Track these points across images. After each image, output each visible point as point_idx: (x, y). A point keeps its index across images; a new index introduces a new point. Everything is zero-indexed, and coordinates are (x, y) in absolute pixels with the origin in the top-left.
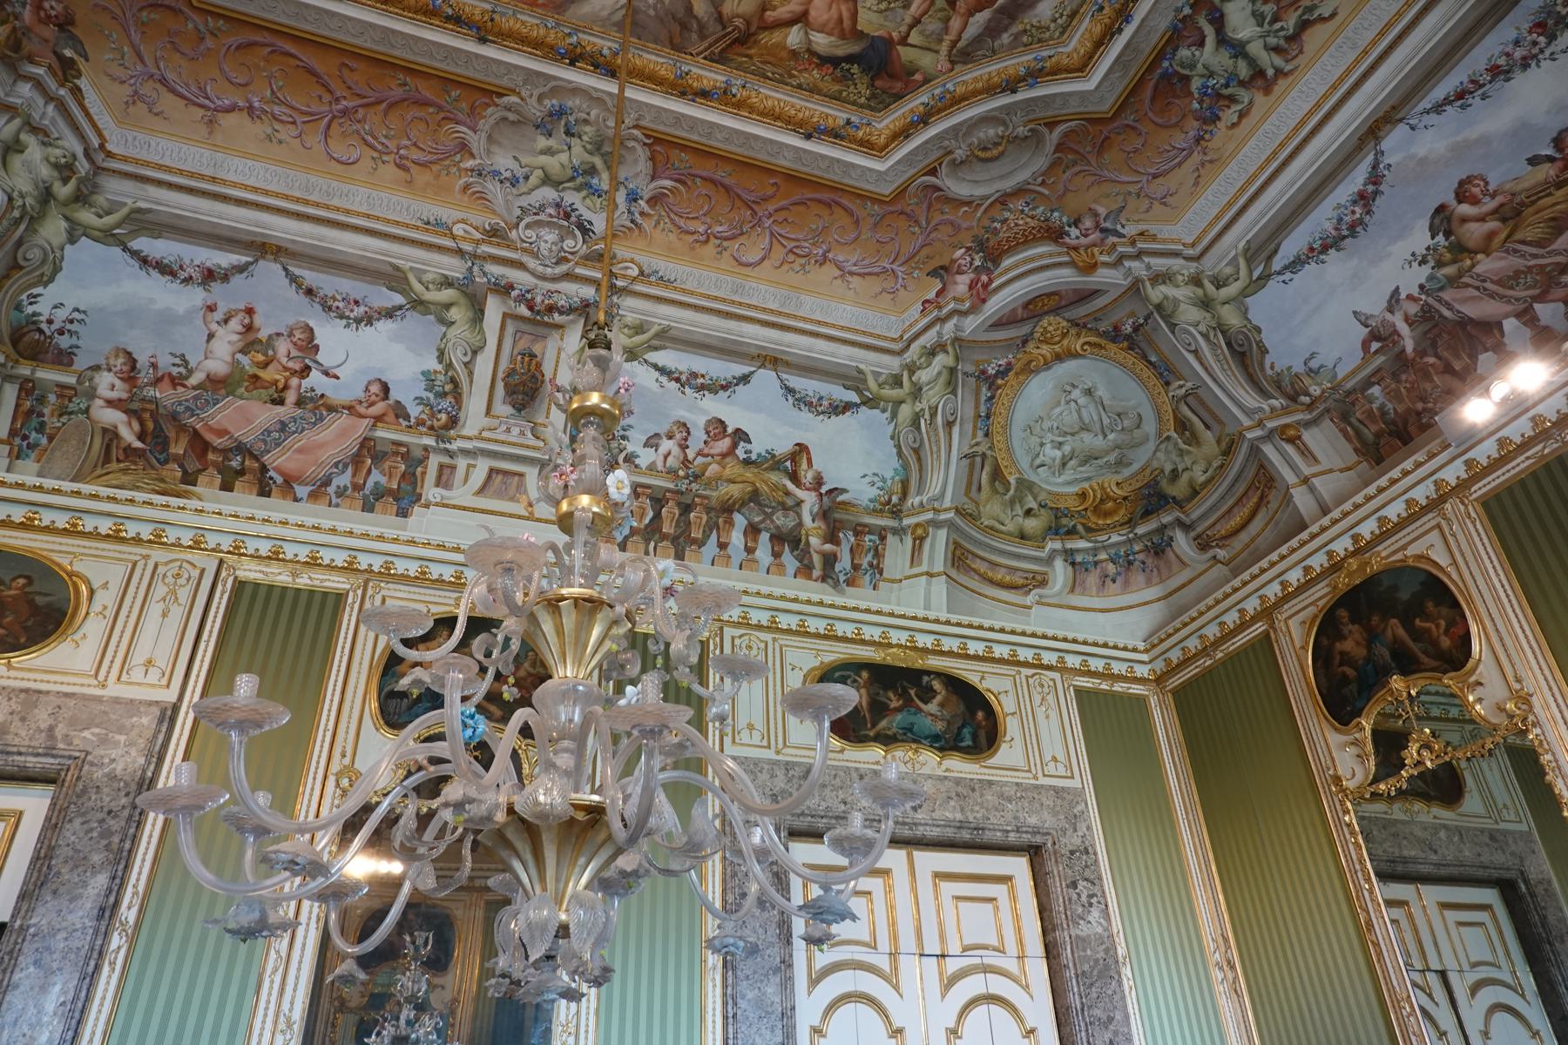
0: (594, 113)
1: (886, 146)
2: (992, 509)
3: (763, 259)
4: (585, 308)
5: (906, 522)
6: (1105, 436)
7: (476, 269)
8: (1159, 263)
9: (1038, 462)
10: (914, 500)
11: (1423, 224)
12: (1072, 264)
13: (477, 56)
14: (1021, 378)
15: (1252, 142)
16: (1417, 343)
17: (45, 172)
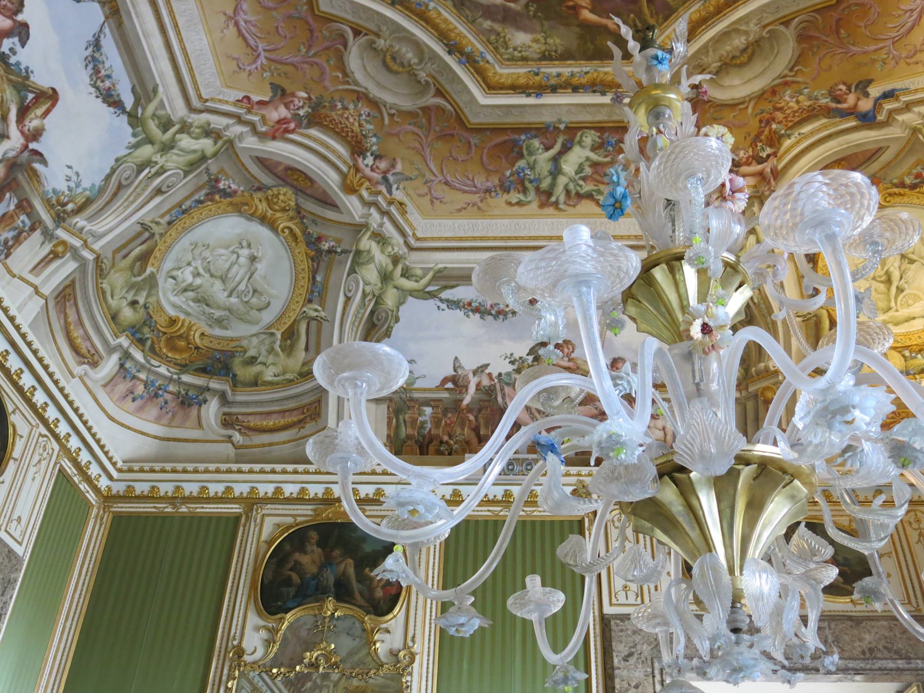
2: (117, 279)
5: (61, 233)
6: (230, 295)
8: (389, 229)
9: (175, 273)
10: (80, 221)
11: (531, 344)
12: (344, 176)
15: (506, 221)
16: (472, 402)
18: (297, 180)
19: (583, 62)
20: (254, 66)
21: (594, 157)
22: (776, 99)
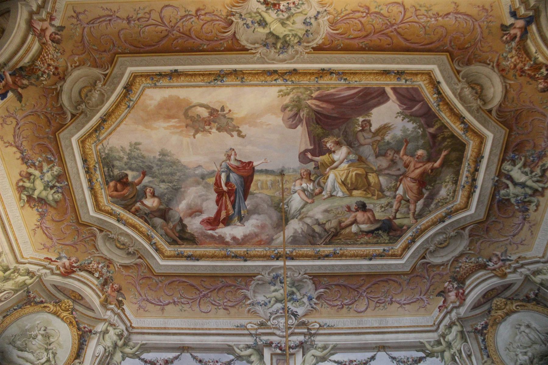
0: (289, 274)
1: (402, 254)
3: (367, 308)
4: (301, 345)
7: (258, 339)
8: (533, 267)
12: (496, 276)
13: (245, 266)
14: (494, 327)
17: (115, 338)
18: (491, 295)
19: (462, 166)
20: (426, 302)
21: (519, 165)
22: (507, 69)
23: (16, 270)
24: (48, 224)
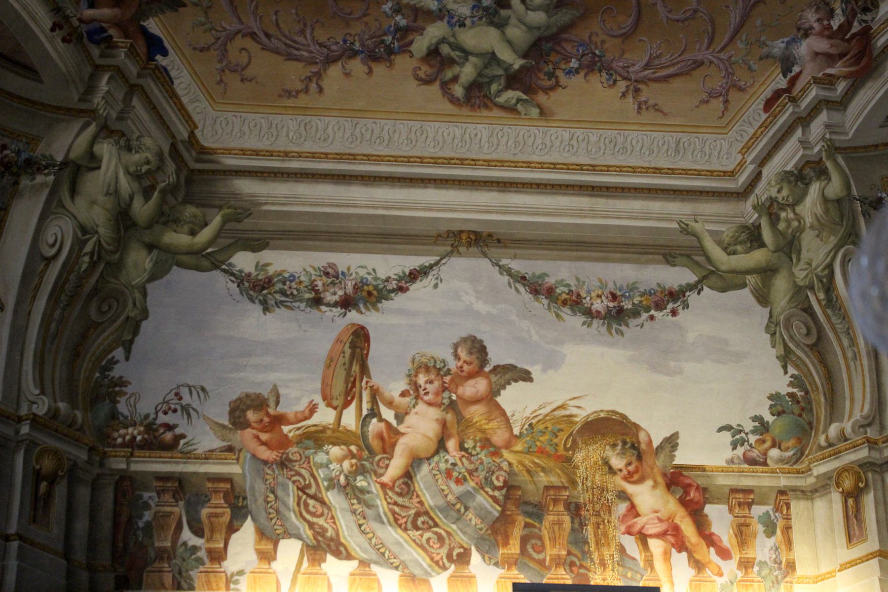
23: (771, 210)
24: (636, 58)
